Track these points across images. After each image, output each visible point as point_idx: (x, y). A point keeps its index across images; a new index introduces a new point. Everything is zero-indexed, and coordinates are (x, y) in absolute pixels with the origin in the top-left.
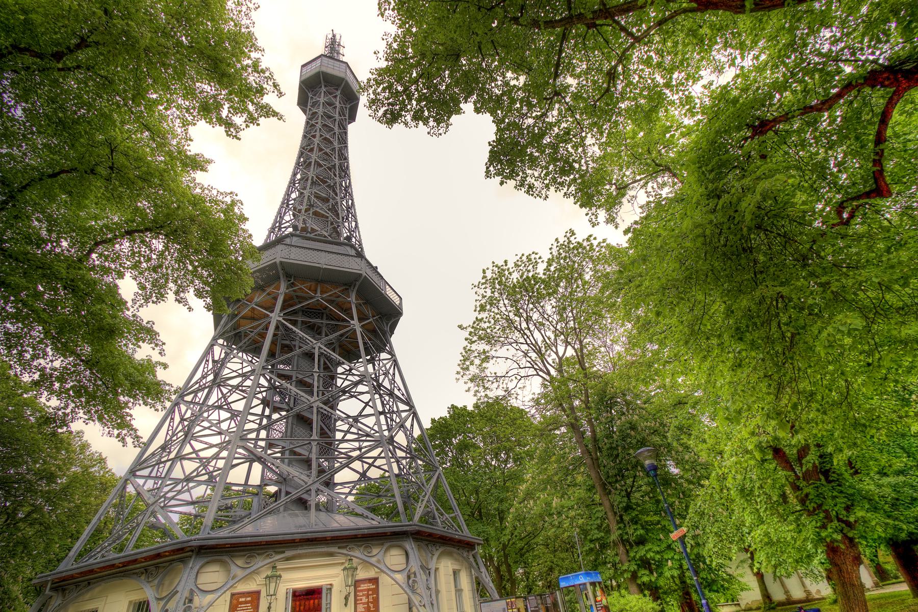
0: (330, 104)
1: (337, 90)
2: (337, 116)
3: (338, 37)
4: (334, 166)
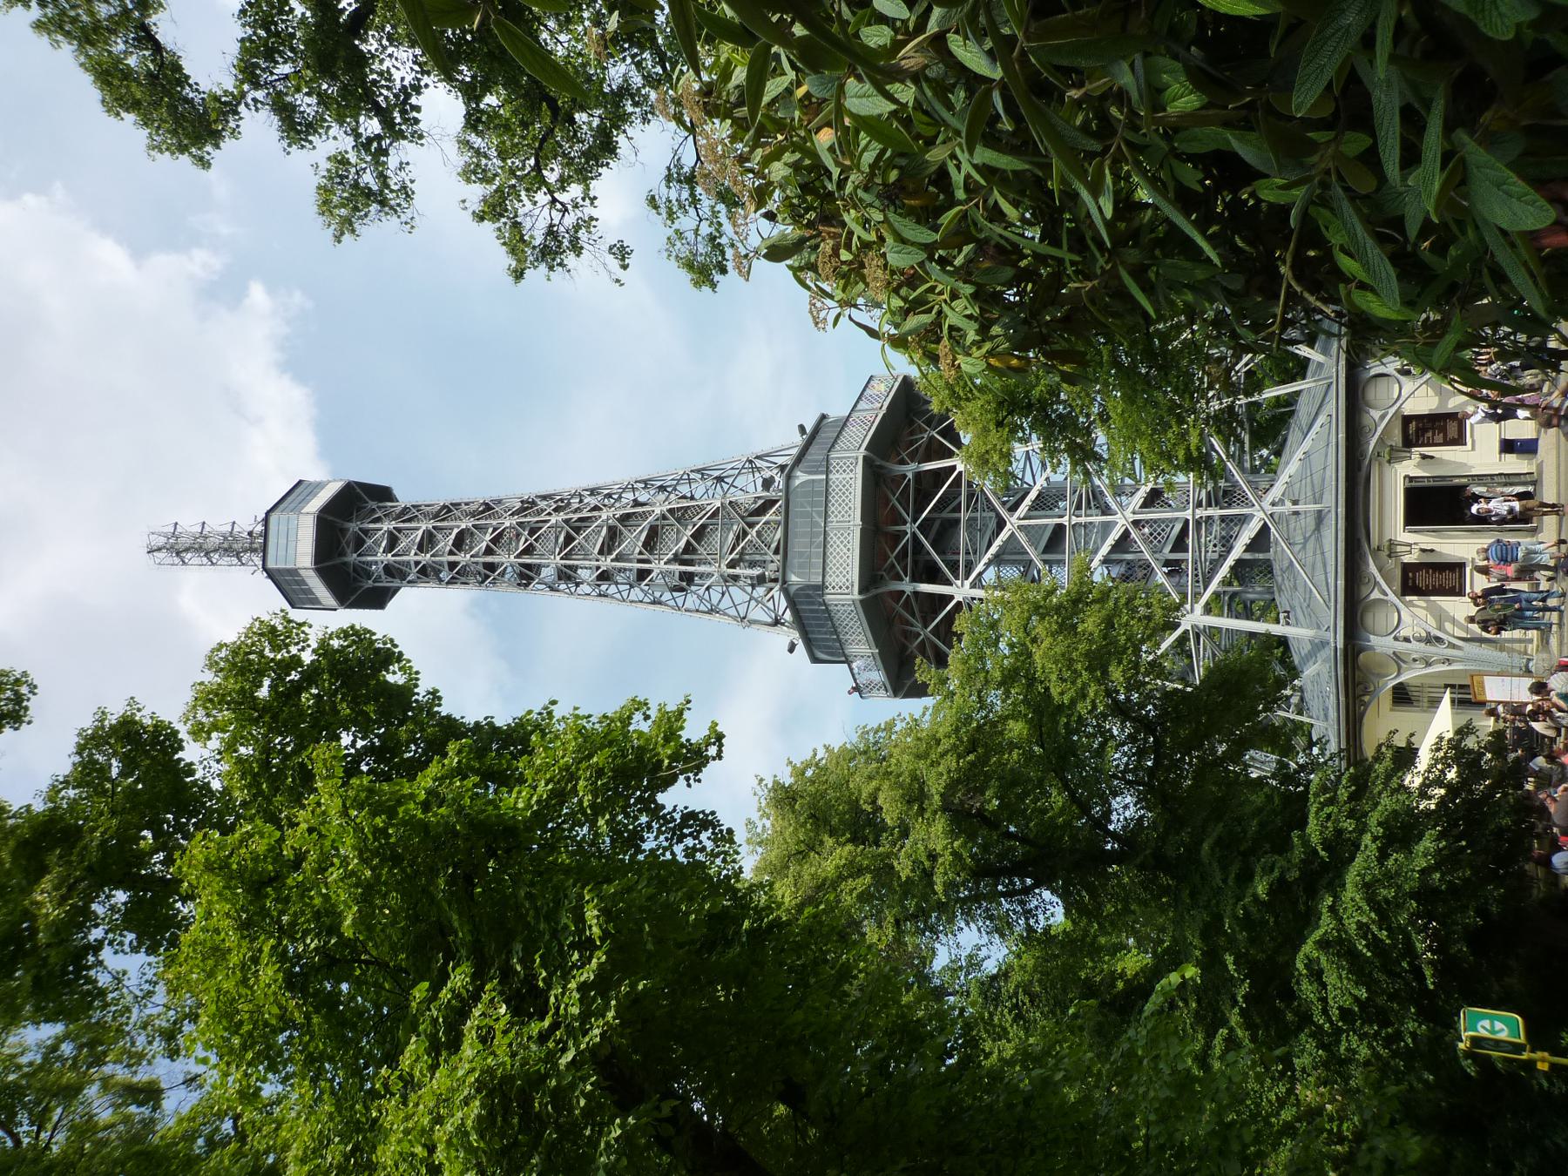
0: (393, 541)
1: (344, 531)
2: (430, 525)
3: (161, 541)
4: (567, 521)
